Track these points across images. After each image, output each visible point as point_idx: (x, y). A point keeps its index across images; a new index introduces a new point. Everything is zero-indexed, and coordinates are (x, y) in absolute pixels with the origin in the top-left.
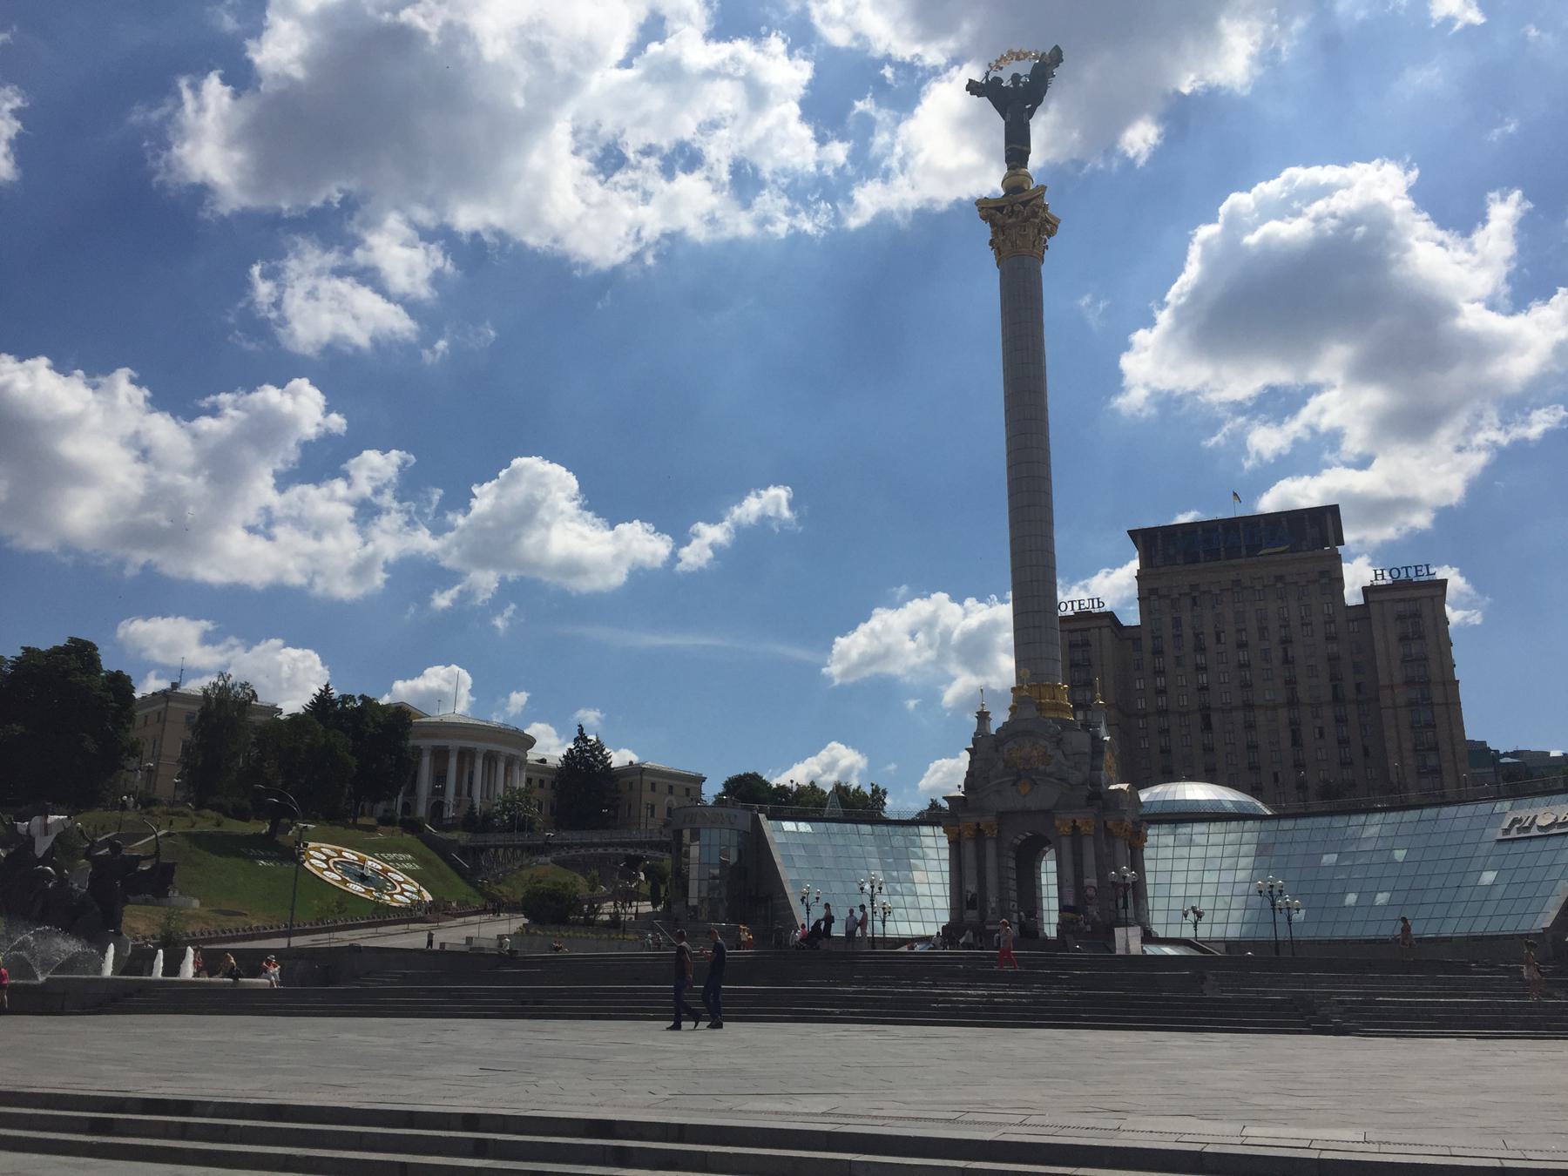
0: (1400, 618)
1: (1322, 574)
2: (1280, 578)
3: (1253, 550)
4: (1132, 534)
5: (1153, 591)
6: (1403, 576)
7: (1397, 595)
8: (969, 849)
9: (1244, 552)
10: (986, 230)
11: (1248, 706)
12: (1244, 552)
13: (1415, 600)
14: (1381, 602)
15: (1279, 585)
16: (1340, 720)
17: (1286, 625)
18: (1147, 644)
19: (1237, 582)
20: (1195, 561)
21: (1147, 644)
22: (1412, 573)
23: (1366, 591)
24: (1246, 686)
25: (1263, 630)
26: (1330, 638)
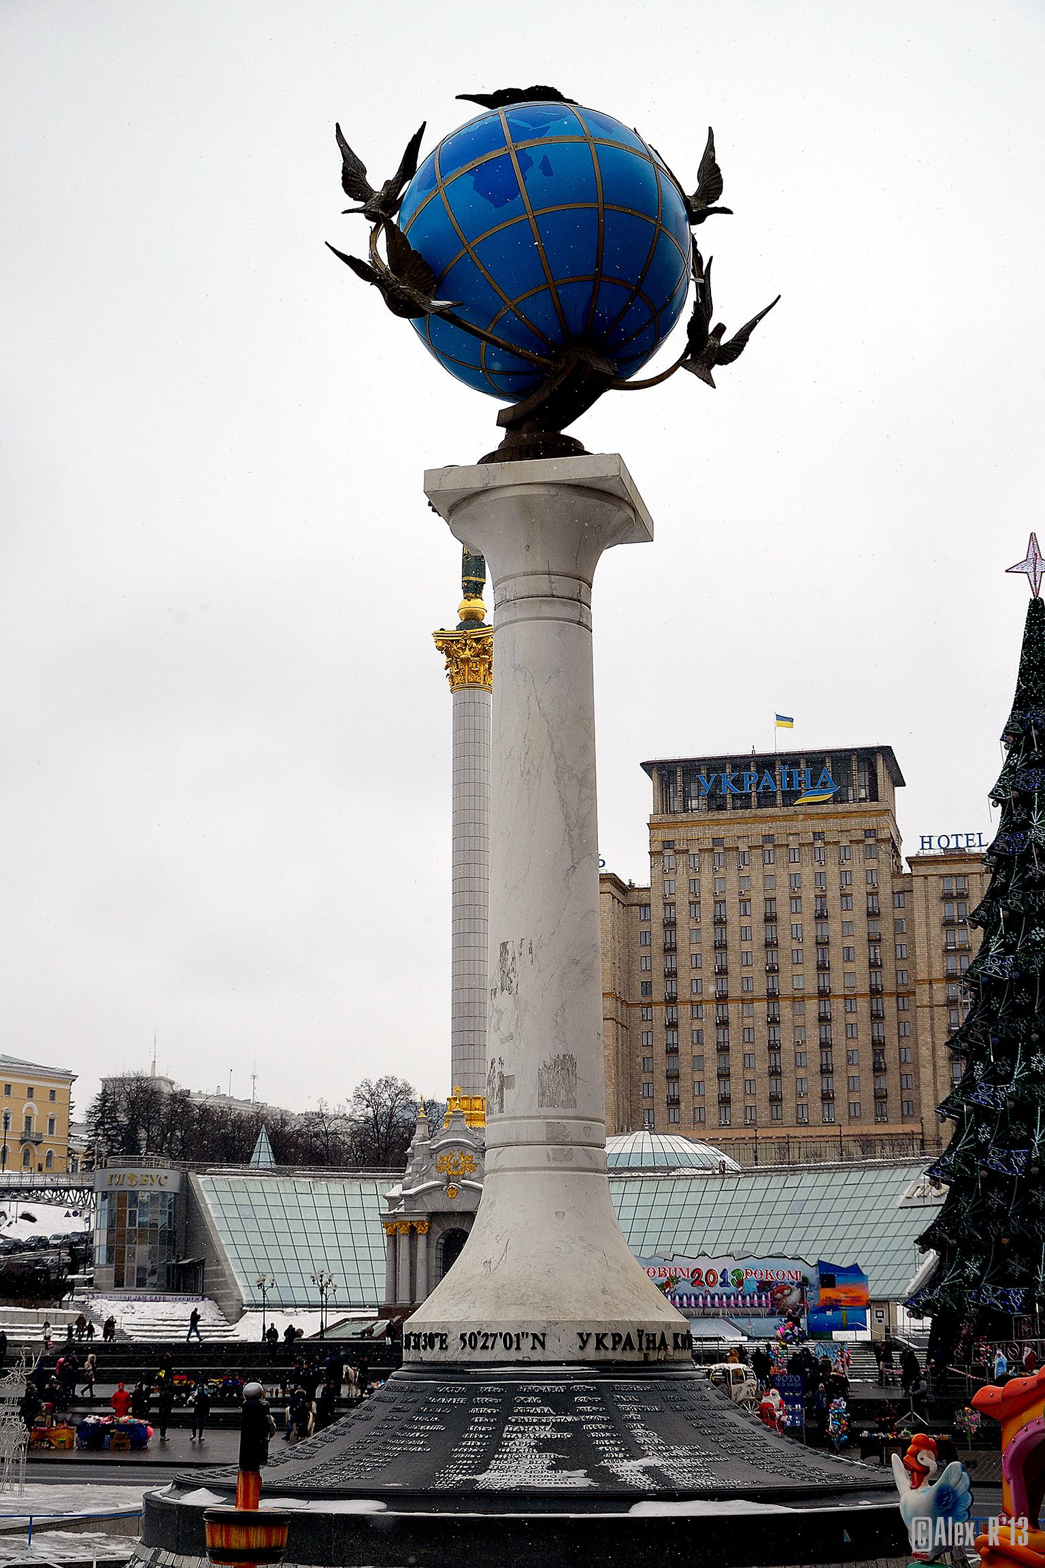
0: (947, 897)
1: (869, 833)
2: (818, 835)
3: (790, 796)
4: (648, 767)
5: (668, 844)
6: (953, 845)
7: (944, 869)
8: (404, 1243)
9: (779, 798)
10: (443, 659)
11: (772, 997)
12: (779, 798)
13: (965, 875)
14: (926, 877)
15: (819, 844)
16: (876, 1017)
17: (822, 897)
18: (657, 911)
19: (768, 838)
20: (721, 807)
21: (657, 911)
22: (962, 844)
23: (912, 861)
24: (772, 970)
25: (795, 898)
26: (873, 914)
